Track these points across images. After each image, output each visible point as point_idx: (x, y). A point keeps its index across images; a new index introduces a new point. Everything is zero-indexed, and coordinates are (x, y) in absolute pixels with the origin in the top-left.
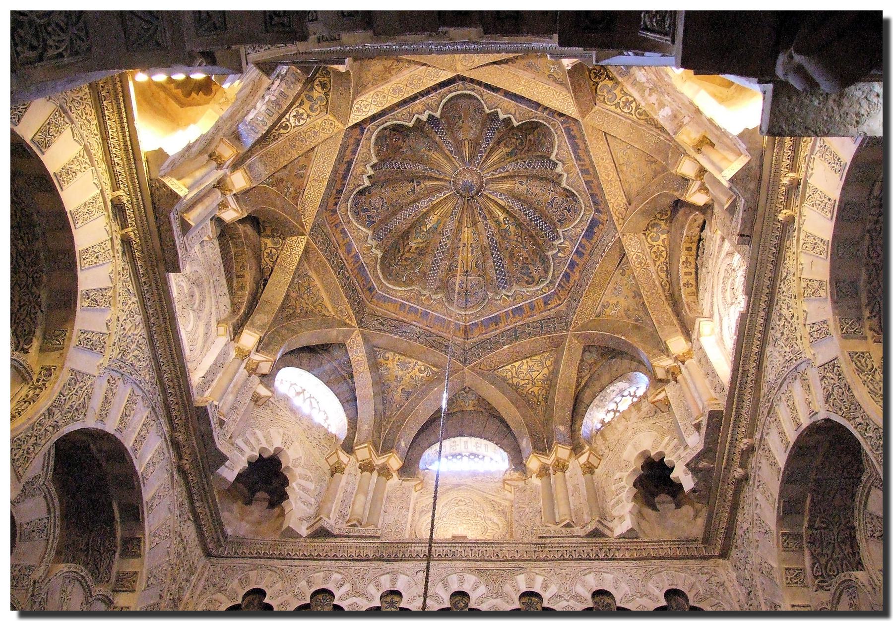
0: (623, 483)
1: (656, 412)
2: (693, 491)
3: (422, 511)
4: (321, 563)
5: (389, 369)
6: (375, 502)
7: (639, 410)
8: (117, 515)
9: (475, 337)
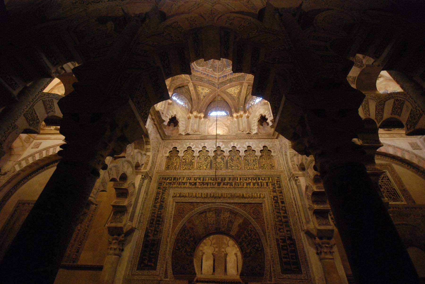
0: (255, 121)
1: (265, 104)
2: (272, 126)
3: (209, 127)
4: (188, 140)
5: (199, 91)
6: (199, 126)
7: (261, 103)
8: (143, 137)
9: (221, 80)
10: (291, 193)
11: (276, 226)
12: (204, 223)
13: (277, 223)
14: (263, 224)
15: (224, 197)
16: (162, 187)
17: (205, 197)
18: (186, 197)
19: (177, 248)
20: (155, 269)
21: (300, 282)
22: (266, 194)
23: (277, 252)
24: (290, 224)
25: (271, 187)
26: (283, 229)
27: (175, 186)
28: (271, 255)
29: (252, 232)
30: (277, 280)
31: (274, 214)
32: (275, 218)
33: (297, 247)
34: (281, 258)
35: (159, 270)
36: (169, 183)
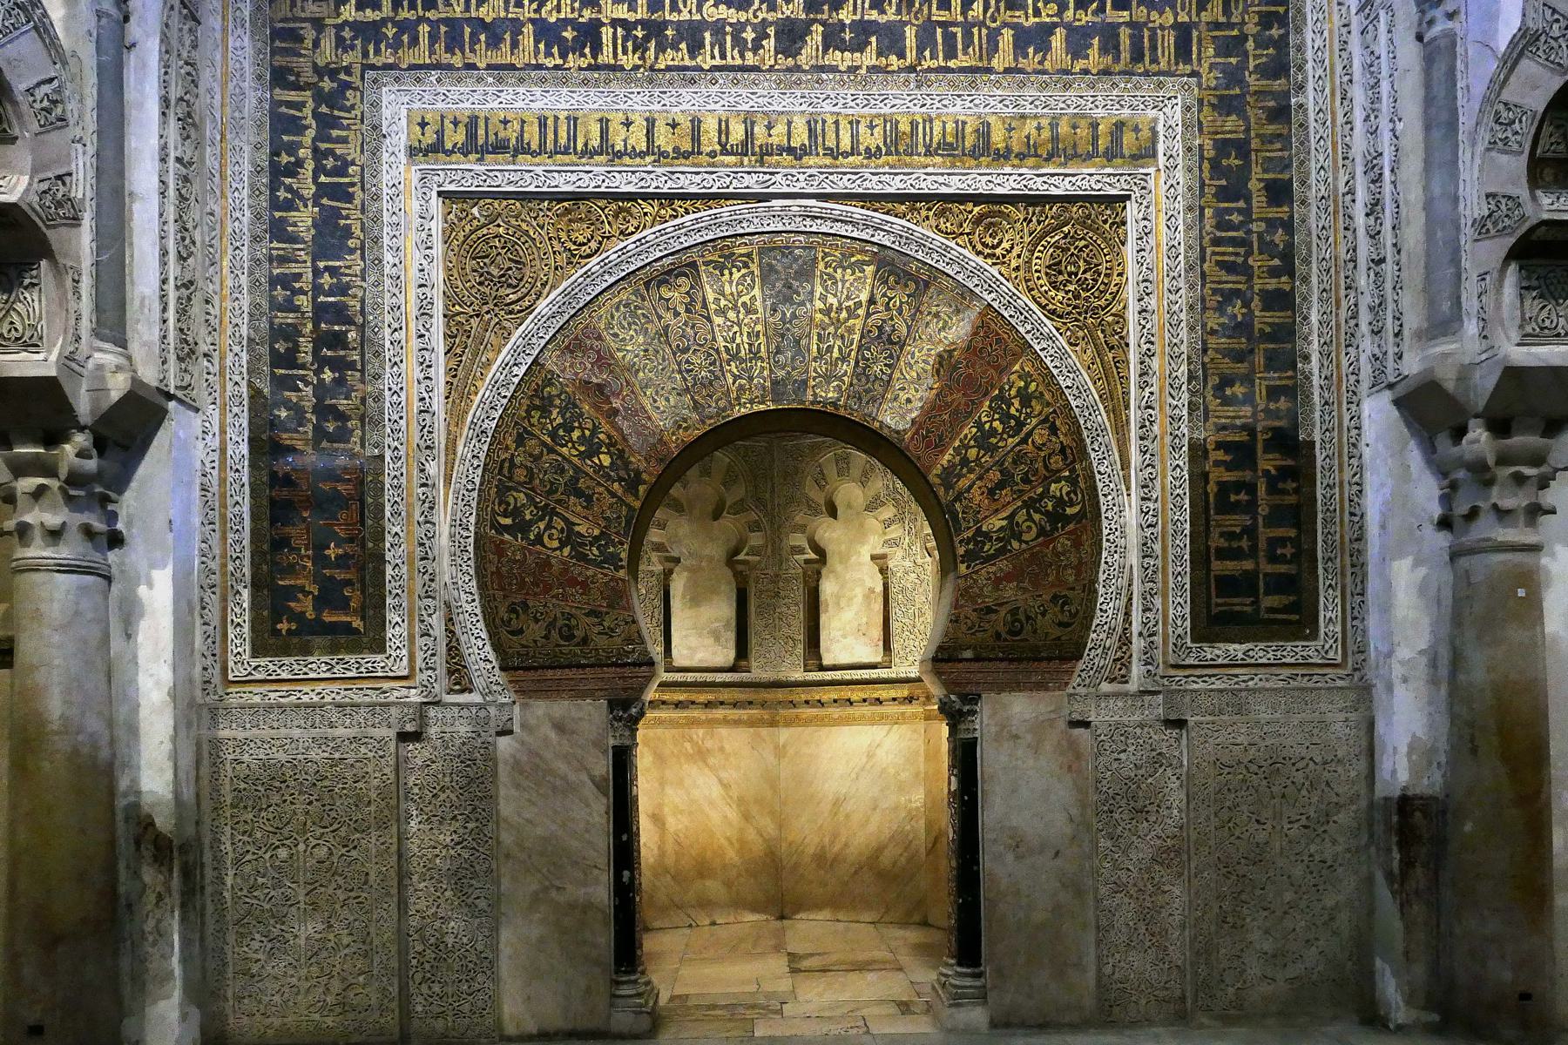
10: (1358, 116)
11: (1204, 364)
12: (685, 350)
13: (1212, 341)
14: (1112, 348)
15: (834, 153)
16: (303, 65)
17: (676, 149)
18: (522, 149)
19: (508, 521)
20: (379, 646)
21: (1293, 677)
22: (1160, 128)
23: (1188, 526)
24: (1299, 342)
25: (1212, 67)
26: (1248, 380)
27: (422, 55)
28: (1144, 544)
29: (1034, 403)
30: (1160, 671)
31: (1203, 275)
32: (1204, 309)
33: (1319, 492)
34: (1200, 559)
35: (404, 652)
36: (359, 28)
